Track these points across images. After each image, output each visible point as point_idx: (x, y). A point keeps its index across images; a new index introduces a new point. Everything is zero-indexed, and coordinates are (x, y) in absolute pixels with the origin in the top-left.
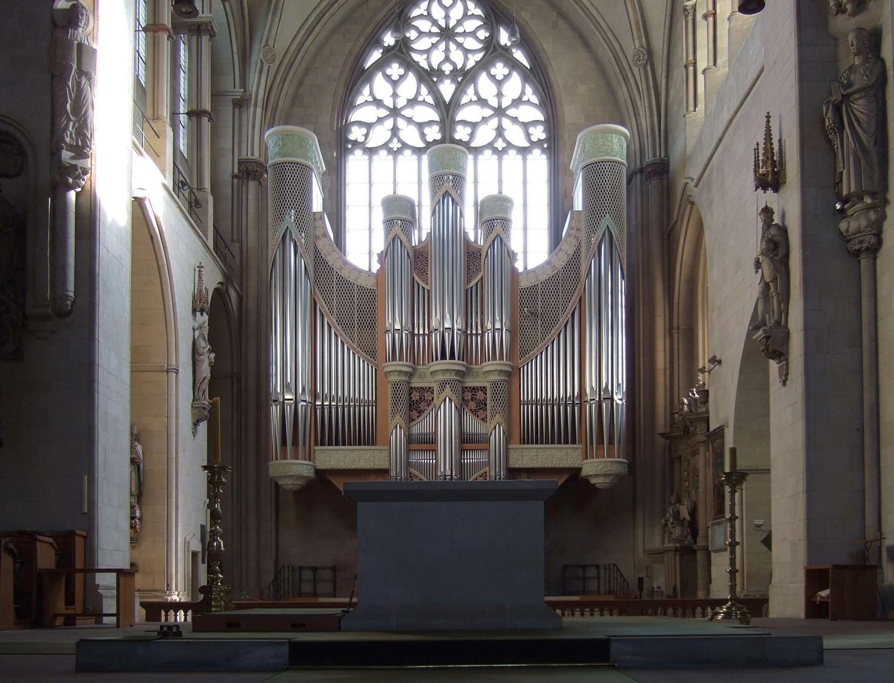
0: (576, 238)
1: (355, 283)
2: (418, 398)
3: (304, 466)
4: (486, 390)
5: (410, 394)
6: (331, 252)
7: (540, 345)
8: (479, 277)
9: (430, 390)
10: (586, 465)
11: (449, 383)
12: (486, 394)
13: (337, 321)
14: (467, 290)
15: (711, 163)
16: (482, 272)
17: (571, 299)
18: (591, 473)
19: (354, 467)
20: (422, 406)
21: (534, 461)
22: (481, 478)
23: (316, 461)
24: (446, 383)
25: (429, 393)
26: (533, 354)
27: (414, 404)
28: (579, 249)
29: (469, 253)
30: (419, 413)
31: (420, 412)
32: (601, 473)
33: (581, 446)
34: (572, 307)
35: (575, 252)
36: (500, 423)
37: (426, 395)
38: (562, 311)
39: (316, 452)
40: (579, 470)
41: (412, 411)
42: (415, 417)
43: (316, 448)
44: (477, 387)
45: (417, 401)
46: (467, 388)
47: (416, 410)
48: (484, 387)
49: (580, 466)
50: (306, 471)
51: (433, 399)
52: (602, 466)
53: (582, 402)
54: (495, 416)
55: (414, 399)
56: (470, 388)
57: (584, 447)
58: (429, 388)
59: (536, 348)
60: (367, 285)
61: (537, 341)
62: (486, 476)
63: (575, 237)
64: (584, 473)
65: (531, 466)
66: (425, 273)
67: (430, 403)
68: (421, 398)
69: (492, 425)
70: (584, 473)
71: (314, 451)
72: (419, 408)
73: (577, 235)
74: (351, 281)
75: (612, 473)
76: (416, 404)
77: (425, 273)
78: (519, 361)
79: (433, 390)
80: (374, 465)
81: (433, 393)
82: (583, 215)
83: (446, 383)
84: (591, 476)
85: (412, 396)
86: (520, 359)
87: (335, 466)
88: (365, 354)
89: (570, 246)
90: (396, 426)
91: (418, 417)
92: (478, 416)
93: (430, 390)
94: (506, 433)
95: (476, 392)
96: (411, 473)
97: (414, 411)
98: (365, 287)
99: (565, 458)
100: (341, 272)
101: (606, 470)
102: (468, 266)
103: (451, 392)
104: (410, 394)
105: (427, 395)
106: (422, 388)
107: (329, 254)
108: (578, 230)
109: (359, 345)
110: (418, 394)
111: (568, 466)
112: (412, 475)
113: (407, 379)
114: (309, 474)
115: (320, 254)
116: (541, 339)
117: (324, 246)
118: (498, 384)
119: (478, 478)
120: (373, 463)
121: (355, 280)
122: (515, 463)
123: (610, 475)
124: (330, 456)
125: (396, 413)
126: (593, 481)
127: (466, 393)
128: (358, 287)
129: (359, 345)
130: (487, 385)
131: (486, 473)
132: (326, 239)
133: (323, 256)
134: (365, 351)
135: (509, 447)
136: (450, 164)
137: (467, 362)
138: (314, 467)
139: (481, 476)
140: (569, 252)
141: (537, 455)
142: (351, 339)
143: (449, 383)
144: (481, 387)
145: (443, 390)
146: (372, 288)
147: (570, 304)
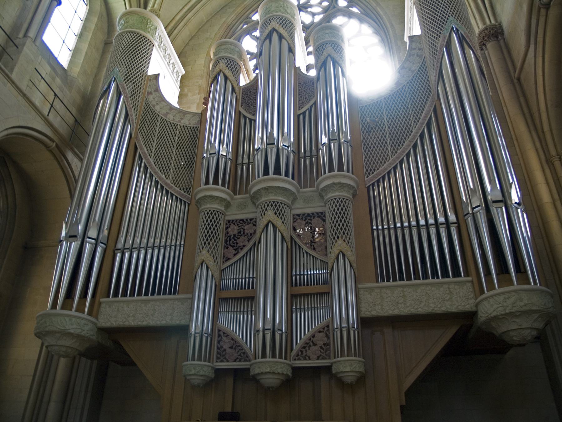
0: (420, 56)
1: (179, 124)
2: (236, 232)
3: (74, 319)
4: (325, 216)
5: (227, 228)
6: (160, 102)
7: (391, 159)
8: (312, 102)
9: (253, 222)
10: (485, 303)
11: (272, 205)
12: (324, 221)
13: (155, 163)
14: (299, 116)
15: (527, 62)
16: (315, 97)
17: (423, 109)
18: (495, 314)
19: (145, 323)
20: (241, 241)
21: (400, 306)
22: (322, 334)
23: (101, 317)
24: (268, 205)
25: (251, 225)
26: (385, 169)
27: (230, 240)
28: (424, 65)
29: (301, 83)
30: (235, 250)
31: (237, 250)
32: (515, 309)
33: (469, 278)
34: (426, 117)
35: (420, 68)
36: (343, 250)
37: (246, 228)
38: (415, 122)
39: (103, 305)
40: (472, 315)
41: (227, 248)
42: (230, 256)
43: (102, 300)
44: (313, 214)
45: (234, 235)
46: (299, 215)
47: (233, 246)
48: (322, 213)
49: (474, 309)
50: (75, 326)
51: (255, 231)
52: (513, 299)
53: (461, 216)
54: (336, 241)
55: (231, 233)
56: (304, 215)
57: (476, 281)
58: (251, 220)
59: (387, 163)
60: (190, 124)
61: (388, 155)
62: (328, 330)
63: (417, 55)
64: (482, 316)
65: (396, 312)
66: (252, 107)
67: (250, 237)
68: (240, 232)
69: (333, 255)
70: (482, 316)
71: (100, 303)
72: (237, 243)
73: (419, 54)
74: (175, 123)
75: (534, 308)
76: (233, 240)
77: (252, 107)
78: (366, 179)
79: (256, 222)
80: (171, 319)
81: (255, 225)
82: (425, 41)
83: (268, 205)
84: (496, 317)
85: (229, 230)
86: (367, 177)
87: (121, 323)
88: (178, 189)
89: (414, 63)
90: (202, 264)
91: (235, 255)
92: (314, 249)
93: (252, 222)
94: (354, 265)
95: (311, 220)
96: (219, 331)
97: (231, 248)
98: (188, 126)
99: (447, 298)
100: (166, 117)
101: (522, 304)
102: (299, 94)
103: (275, 216)
104: (227, 228)
105: (248, 229)
106: (242, 220)
107: (157, 104)
108: (419, 49)
109: (174, 181)
110: (236, 228)
111: (453, 309)
112: (221, 333)
113: (222, 208)
114: (80, 331)
115: (149, 105)
116: (392, 153)
117: (153, 99)
118: (338, 202)
119: (317, 335)
120: (170, 317)
121: (180, 121)
122: (369, 311)
123: (535, 312)
124: (118, 310)
125: (203, 248)
126: (502, 328)
127: (299, 221)
128: (181, 127)
129: (174, 181)
130: (326, 209)
131: (328, 326)
132: (157, 93)
133: (151, 106)
134: (179, 186)
135: (360, 286)
136: (277, 10)
137: (299, 183)
138: (95, 324)
139: (320, 332)
140: (413, 69)
141: (404, 296)
142: (166, 176)
143: (272, 205)
144: (317, 213)
145: (264, 214)
146: (195, 126)
147: (423, 115)
